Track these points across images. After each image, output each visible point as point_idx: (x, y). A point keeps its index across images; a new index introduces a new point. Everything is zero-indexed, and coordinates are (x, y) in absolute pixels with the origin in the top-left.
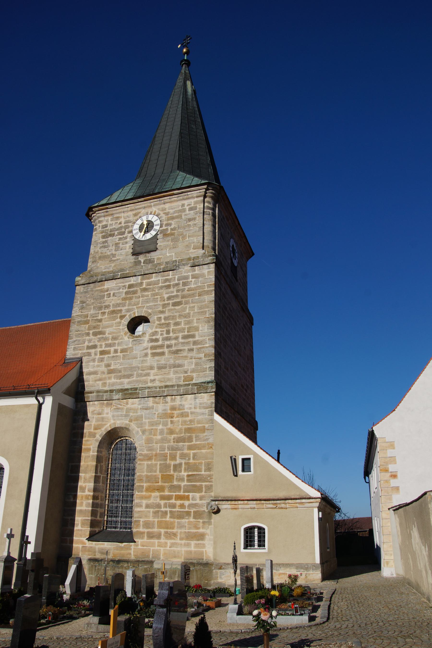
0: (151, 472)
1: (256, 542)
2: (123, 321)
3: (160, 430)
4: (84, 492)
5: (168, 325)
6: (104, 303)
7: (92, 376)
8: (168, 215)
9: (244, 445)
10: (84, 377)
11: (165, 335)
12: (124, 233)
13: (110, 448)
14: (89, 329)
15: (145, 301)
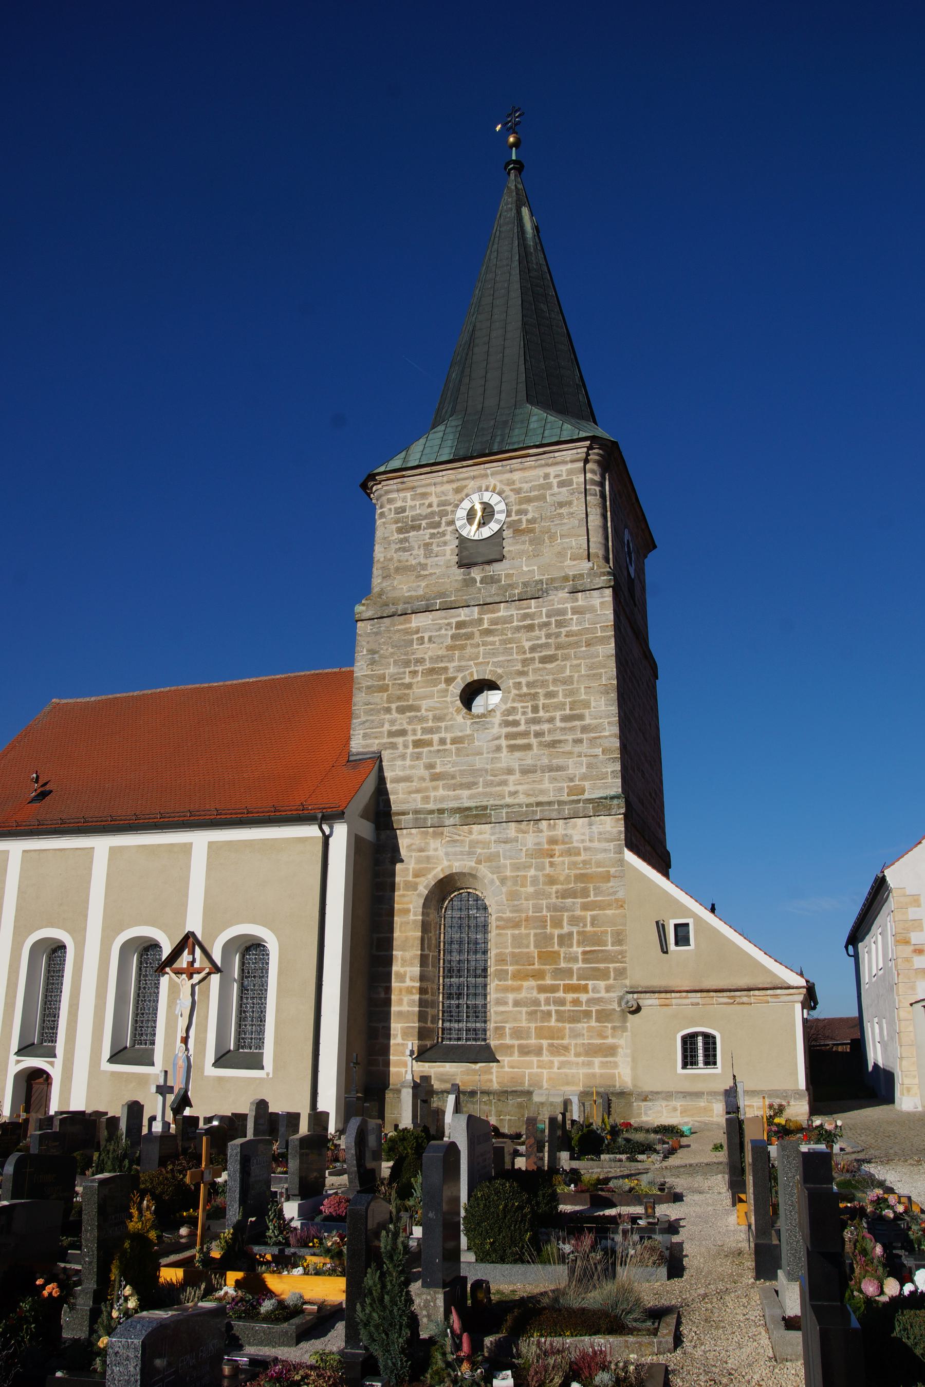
0: (519, 947)
1: (701, 1058)
2: (451, 688)
3: (531, 877)
4: (404, 982)
5: (535, 696)
6: (413, 654)
7: (402, 785)
8: (519, 493)
9: (677, 902)
10: (388, 786)
11: (530, 715)
12: (438, 525)
13: (442, 908)
14: (389, 701)
15: (489, 653)
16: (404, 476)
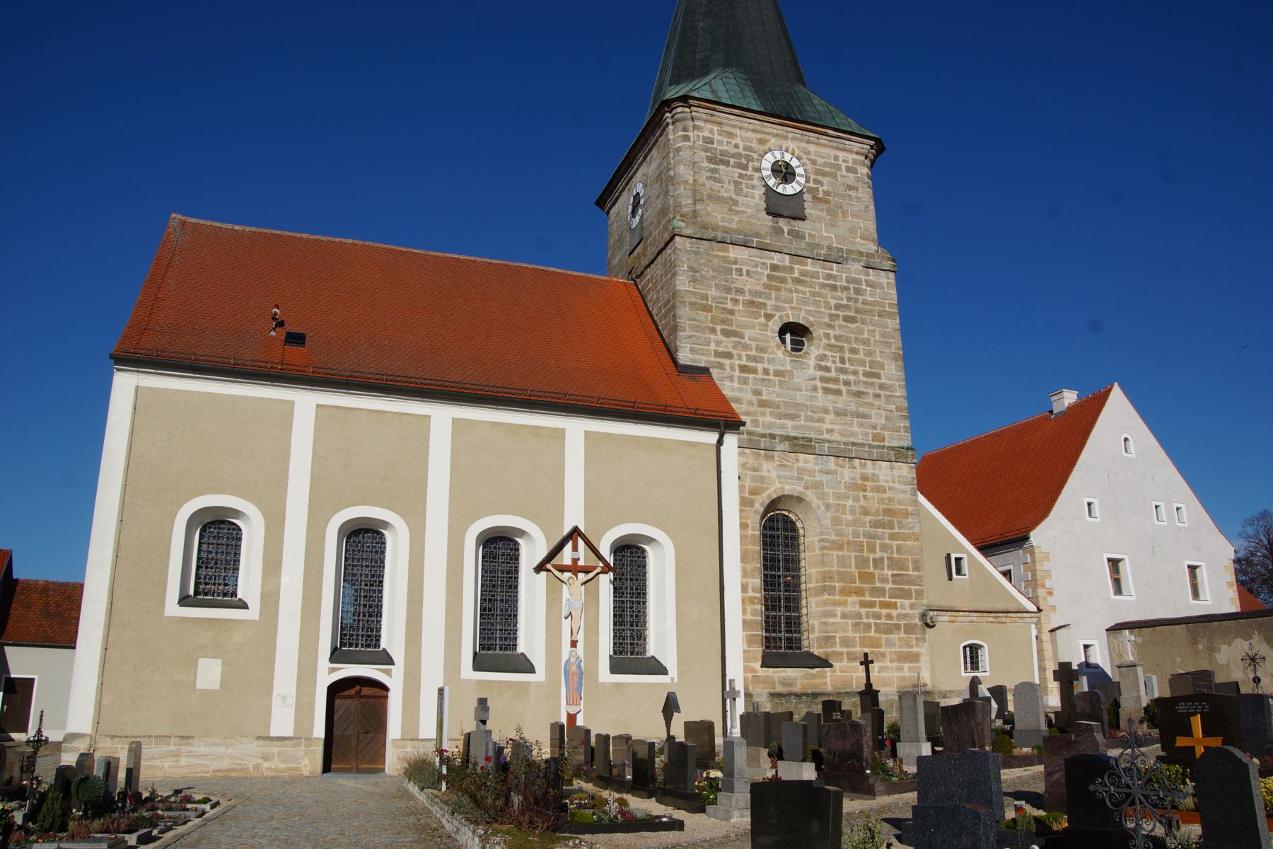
2: (770, 324)
11: (839, 365)
12: (745, 168)
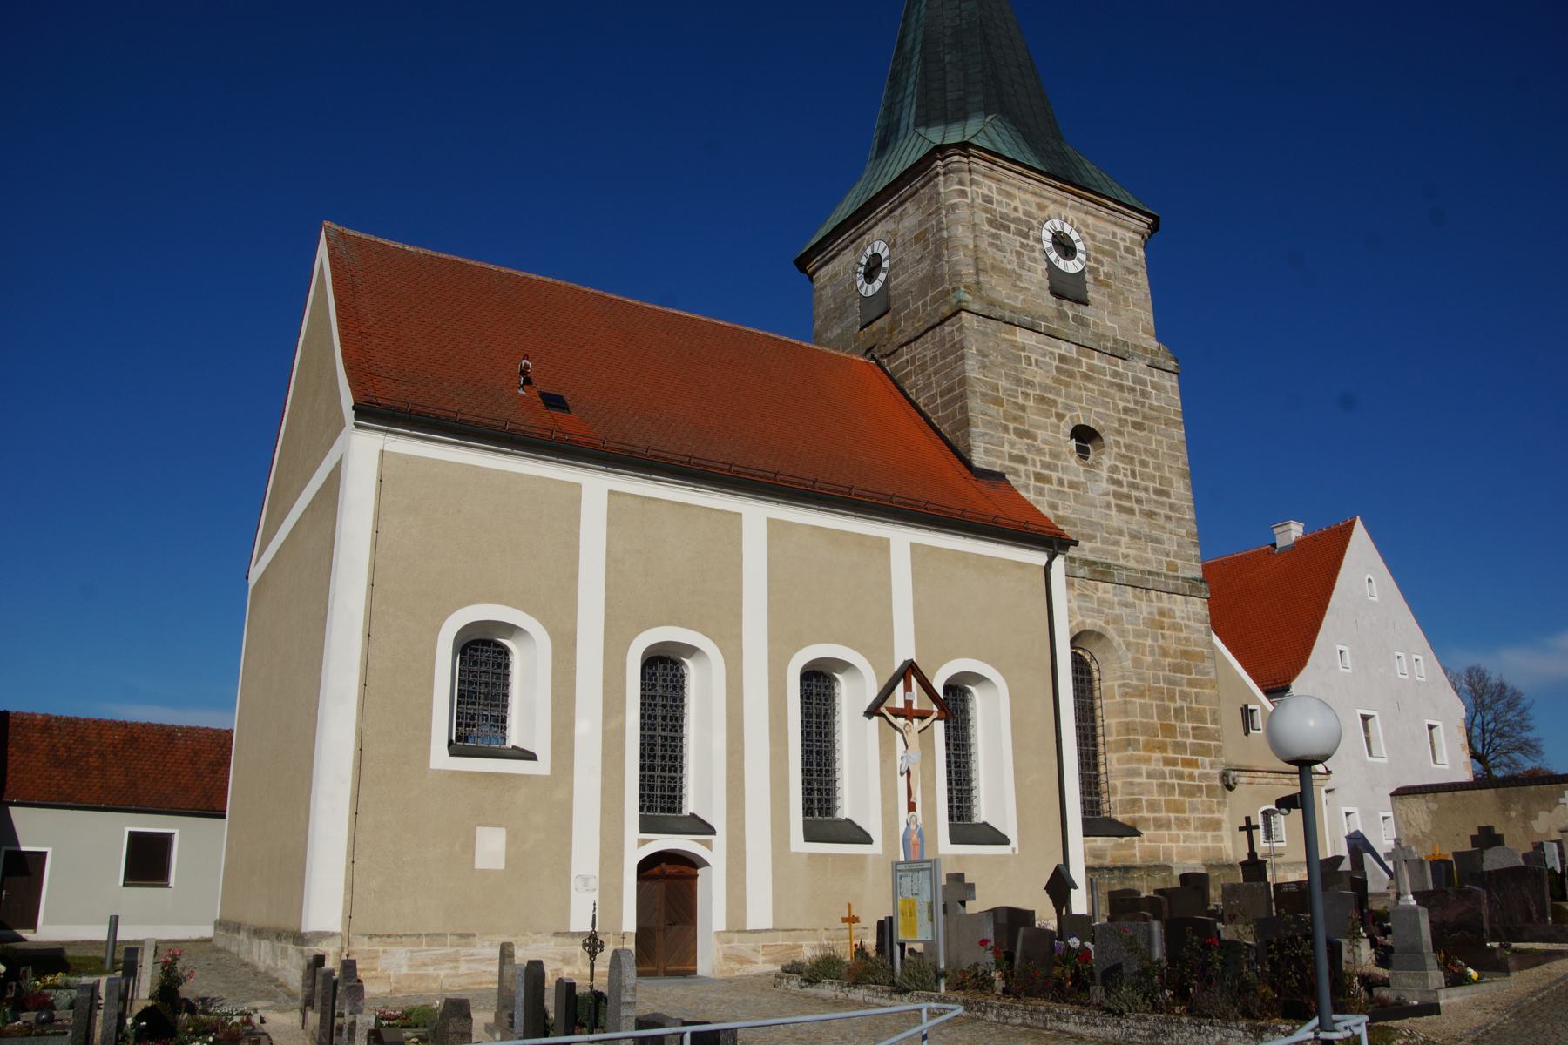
12: (1026, 236)
16: (994, 163)
